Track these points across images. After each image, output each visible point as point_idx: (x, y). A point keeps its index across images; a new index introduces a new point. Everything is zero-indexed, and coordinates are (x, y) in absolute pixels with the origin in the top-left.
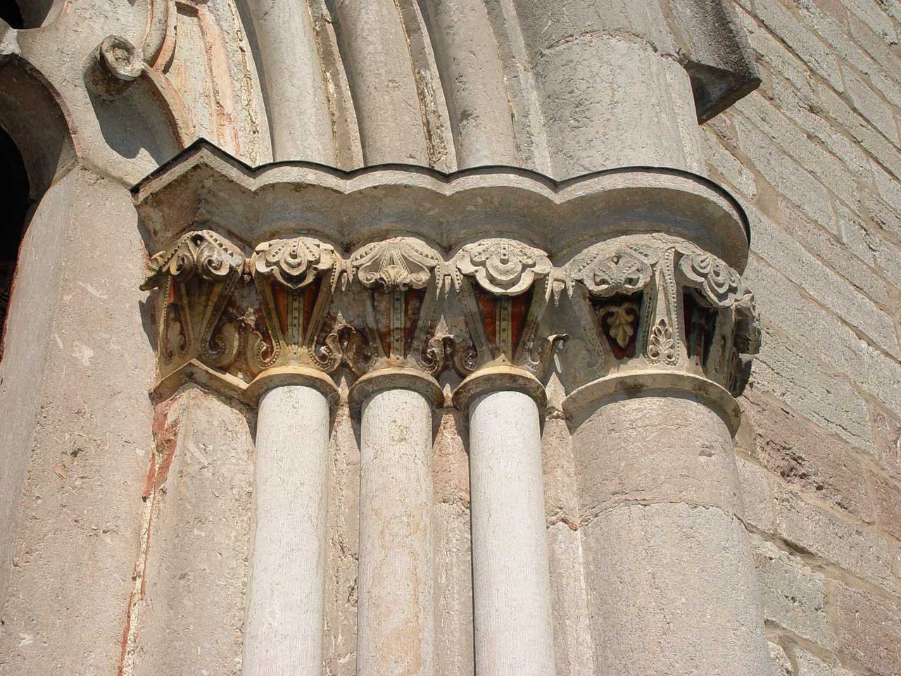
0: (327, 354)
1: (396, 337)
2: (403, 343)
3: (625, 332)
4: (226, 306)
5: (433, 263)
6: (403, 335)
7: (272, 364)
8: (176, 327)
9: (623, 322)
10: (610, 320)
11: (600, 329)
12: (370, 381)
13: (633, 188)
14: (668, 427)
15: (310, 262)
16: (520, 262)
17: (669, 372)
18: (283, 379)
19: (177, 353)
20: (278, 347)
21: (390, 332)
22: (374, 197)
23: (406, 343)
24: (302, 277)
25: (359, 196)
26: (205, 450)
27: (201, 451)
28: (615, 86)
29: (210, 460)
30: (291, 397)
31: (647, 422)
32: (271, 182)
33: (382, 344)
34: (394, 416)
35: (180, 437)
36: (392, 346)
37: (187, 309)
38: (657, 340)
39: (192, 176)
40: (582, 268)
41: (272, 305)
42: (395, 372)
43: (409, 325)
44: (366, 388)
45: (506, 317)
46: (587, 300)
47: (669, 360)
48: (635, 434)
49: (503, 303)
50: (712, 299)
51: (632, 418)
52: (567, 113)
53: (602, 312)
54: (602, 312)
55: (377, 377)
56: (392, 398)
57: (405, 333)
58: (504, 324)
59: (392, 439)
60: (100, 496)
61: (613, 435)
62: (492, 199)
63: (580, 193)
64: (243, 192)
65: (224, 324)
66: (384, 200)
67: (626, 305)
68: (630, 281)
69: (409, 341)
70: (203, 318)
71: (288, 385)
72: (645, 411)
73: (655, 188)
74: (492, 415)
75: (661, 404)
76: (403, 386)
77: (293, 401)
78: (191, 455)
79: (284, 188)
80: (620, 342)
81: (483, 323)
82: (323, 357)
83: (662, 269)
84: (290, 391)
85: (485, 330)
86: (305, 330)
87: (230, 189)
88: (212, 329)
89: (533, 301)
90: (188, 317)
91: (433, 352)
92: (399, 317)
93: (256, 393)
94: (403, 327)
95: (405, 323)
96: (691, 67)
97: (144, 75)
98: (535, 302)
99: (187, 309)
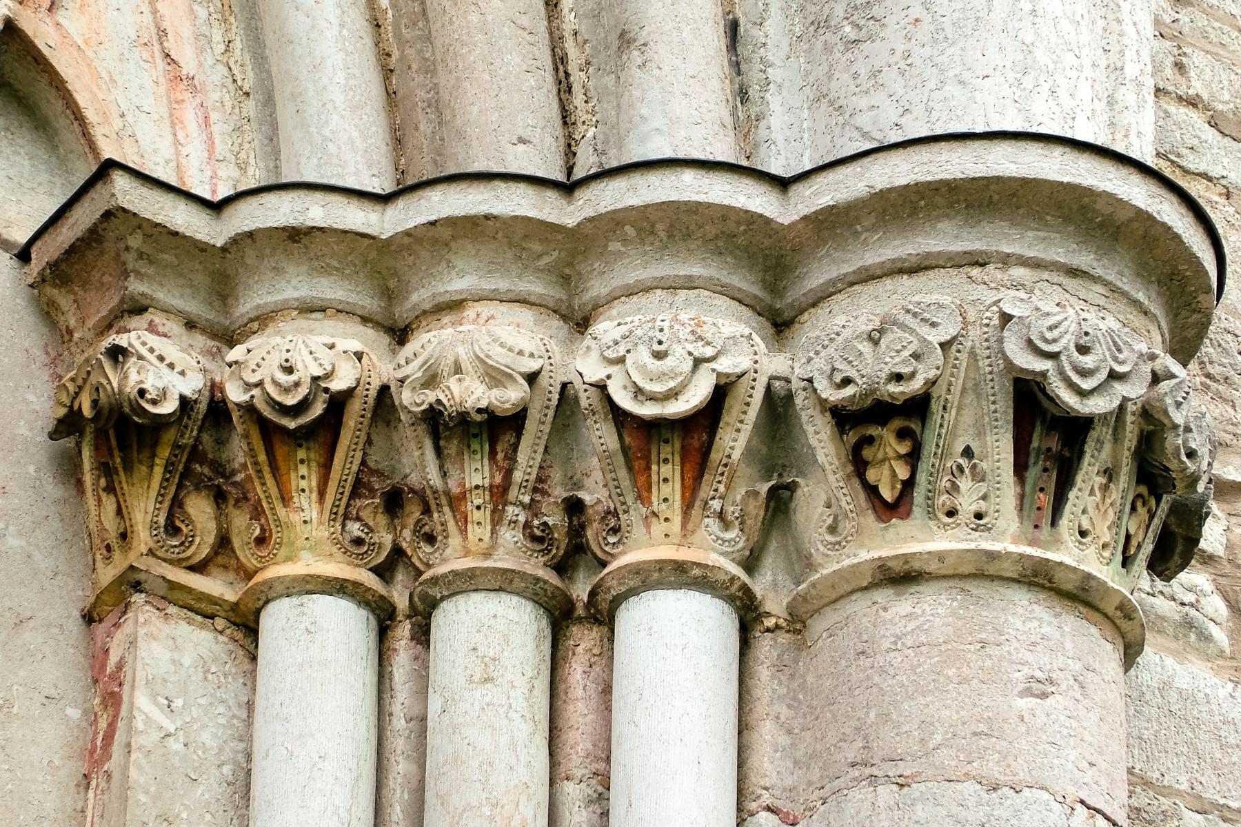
0: (363, 536)
1: (478, 502)
2: (488, 513)
3: (894, 474)
4: (189, 461)
6: (487, 498)
8: (109, 504)
9: (891, 454)
10: (867, 453)
11: (850, 468)
12: (434, 581)
13: (929, 182)
17: (972, 546)
18: (288, 585)
19: (116, 548)
20: (279, 529)
21: (465, 492)
22: (435, 241)
23: (493, 512)
25: (406, 240)
27: (162, 711)
29: (179, 723)
30: (304, 614)
31: (923, 638)
32: (246, 229)
33: (455, 517)
34: (473, 641)
35: (126, 688)
36: (469, 519)
37: (122, 473)
41: (262, 458)
42: (471, 565)
43: (498, 479)
45: (670, 457)
46: (828, 414)
47: (978, 522)
48: (899, 659)
49: (663, 431)
51: (898, 631)
53: (852, 437)
54: (852, 437)
55: (445, 576)
56: (471, 609)
57: (492, 496)
58: (666, 470)
59: (470, 680)
60: (9, 786)
61: (861, 663)
62: (653, 226)
63: (825, 200)
64: (202, 250)
65: (189, 492)
66: (453, 244)
67: (897, 423)
69: (500, 507)
70: (149, 487)
71: (300, 593)
72: (922, 619)
73: (974, 179)
74: (642, 633)
75: (955, 604)
76: (489, 587)
77: (306, 621)
78: (144, 717)
79: (270, 237)
80: (887, 494)
81: (630, 469)
82: (358, 542)
83: (972, 348)
85: (634, 482)
86: (322, 494)
87: (177, 248)
88: (166, 504)
89: (721, 425)
90: (125, 487)
91: (545, 524)
92: (480, 467)
93: (253, 606)
95: (492, 476)
98: (728, 424)
99: (122, 473)
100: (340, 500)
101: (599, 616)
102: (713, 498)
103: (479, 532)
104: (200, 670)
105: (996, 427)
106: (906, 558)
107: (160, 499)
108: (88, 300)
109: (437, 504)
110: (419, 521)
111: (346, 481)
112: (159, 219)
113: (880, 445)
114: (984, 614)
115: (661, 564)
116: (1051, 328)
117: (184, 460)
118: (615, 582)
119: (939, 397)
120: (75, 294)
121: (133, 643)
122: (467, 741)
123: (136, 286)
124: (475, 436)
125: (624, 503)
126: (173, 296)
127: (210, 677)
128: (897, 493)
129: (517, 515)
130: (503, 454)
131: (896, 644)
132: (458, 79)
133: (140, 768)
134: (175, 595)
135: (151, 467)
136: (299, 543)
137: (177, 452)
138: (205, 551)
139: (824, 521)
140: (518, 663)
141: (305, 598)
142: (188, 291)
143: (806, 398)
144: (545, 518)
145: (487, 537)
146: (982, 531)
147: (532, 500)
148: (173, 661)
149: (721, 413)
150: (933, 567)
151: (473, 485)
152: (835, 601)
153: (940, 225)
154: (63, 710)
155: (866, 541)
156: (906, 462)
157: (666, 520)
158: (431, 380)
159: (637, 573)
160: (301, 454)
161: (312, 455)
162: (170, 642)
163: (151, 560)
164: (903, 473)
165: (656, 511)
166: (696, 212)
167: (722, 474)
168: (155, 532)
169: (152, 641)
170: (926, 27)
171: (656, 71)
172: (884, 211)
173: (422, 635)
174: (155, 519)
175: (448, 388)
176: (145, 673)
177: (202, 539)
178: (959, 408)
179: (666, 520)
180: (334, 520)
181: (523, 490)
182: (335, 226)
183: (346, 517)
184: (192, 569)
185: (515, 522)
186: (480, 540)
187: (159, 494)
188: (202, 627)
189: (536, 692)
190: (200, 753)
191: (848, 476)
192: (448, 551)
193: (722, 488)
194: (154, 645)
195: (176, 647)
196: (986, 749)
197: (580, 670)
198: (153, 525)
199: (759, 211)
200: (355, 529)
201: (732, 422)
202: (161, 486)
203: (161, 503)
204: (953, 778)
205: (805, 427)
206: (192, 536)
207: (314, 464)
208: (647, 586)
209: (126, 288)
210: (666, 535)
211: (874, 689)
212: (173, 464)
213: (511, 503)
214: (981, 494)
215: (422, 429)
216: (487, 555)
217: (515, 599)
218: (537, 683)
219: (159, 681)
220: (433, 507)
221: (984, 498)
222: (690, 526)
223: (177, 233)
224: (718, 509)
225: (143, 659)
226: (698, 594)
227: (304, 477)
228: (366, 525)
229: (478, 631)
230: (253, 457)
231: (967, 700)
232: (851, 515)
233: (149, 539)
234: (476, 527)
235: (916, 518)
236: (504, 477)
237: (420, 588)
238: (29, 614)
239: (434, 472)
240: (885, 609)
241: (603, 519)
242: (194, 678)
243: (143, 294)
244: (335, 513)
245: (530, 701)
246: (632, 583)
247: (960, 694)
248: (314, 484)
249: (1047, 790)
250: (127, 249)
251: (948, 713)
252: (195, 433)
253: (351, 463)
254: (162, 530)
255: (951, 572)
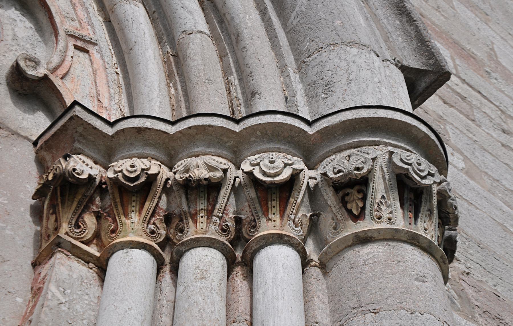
0: (155, 230)
1: (202, 214)
3: (357, 205)
5: (226, 167)
7: (117, 237)
8: (53, 218)
10: (347, 198)
11: (341, 205)
12: (183, 244)
14: (391, 263)
15: (143, 170)
16: (283, 162)
20: (121, 226)
23: (208, 219)
24: (137, 178)
25: (180, 135)
26: (64, 292)
27: (61, 293)
28: (350, 72)
29: (67, 299)
31: (375, 260)
34: (197, 264)
36: (198, 221)
37: (60, 205)
38: (381, 209)
39: (69, 125)
40: (325, 166)
41: (118, 200)
43: (210, 208)
44: (181, 249)
46: (331, 187)
48: (367, 268)
50: (415, 179)
51: (365, 258)
52: (320, 91)
53: (341, 194)
54: (341, 194)
56: (197, 253)
58: (274, 203)
62: (267, 132)
64: (104, 137)
66: (196, 136)
67: (357, 187)
68: (358, 169)
74: (266, 261)
75: (385, 248)
76: (205, 245)
77: (129, 258)
78: (52, 294)
80: (355, 212)
81: (260, 204)
84: (128, 252)
85: (262, 209)
89: (294, 189)
91: (227, 225)
92: (203, 202)
94: (205, 209)
95: (208, 206)
96: (404, 69)
97: (46, 76)
98: (296, 189)
99: (60, 205)
100: (147, 216)
101: (246, 262)
102: (291, 214)
104: (80, 280)
105: (392, 189)
106: (365, 232)
107: (74, 214)
108: (58, 155)
109: (186, 217)
110: (177, 224)
111: (150, 209)
112: (90, 122)
113: (351, 195)
114: (397, 252)
116: (407, 156)
117: (86, 201)
118: (254, 244)
119: (371, 179)
120: (53, 153)
121: (53, 266)
122: (194, 301)
123: (77, 145)
124: (202, 192)
125: (258, 216)
126: (91, 152)
127: (84, 284)
128: (359, 212)
129: (217, 220)
130: (212, 200)
131: (365, 263)
132: (198, 103)
133: (46, 314)
135: (72, 202)
136: (128, 231)
137: (84, 197)
138: (89, 236)
139: (332, 225)
140: (215, 273)
141: (129, 250)
142: (96, 151)
143: (323, 184)
144: (227, 223)
145: (204, 228)
146: (391, 224)
147: (222, 216)
148: (69, 275)
149: (293, 186)
150: (376, 235)
151: (200, 208)
152: (338, 253)
153: (363, 133)
154: (15, 298)
155: (349, 230)
156: (362, 201)
157: (274, 221)
158: (187, 171)
159: (264, 239)
160: (134, 198)
161: (138, 199)
162: (69, 268)
163: (66, 236)
164: (361, 205)
165: (270, 218)
166: (281, 127)
167: (294, 206)
168: (70, 226)
169: (61, 266)
171: (264, 99)
172: (345, 129)
173: (175, 271)
174: (71, 221)
175: (194, 172)
176: (56, 277)
177: (89, 231)
179: (274, 221)
180: (144, 223)
181: (219, 211)
182: (154, 128)
184: (82, 242)
185: (216, 223)
186: (202, 229)
187: (74, 212)
188: (84, 265)
189: (222, 285)
190: (74, 313)
191: (340, 207)
192: (189, 233)
193: (294, 211)
194: (62, 267)
195: (71, 270)
196: (407, 298)
197: (239, 281)
199: (302, 128)
200: (152, 227)
201: (297, 189)
202: (75, 209)
203: (74, 215)
204: (396, 309)
205: (323, 193)
206: (85, 230)
207: (138, 202)
208: (267, 245)
209: (73, 146)
210: (274, 227)
211: (359, 279)
212: (81, 202)
213: (215, 216)
214: (389, 211)
215: (181, 191)
217: (215, 250)
218: (222, 282)
219: (61, 281)
220: (184, 218)
221: (391, 213)
222: (283, 223)
223: (96, 128)
224: (293, 218)
225: (56, 271)
226: (287, 247)
228: (156, 226)
229: (200, 261)
230: (114, 200)
231: (396, 280)
232: (342, 221)
233: (67, 228)
234: (201, 224)
235: (367, 220)
236: (212, 207)
237: (176, 248)
238: (9, 259)
239: (185, 206)
240: (359, 252)
241: (249, 223)
242: (77, 283)
243: (79, 148)
244: (145, 220)
245: (220, 288)
246: (261, 244)
247: (393, 278)
248: (138, 209)
249: (433, 315)
250: (76, 132)
251: (389, 285)
252: (92, 192)
253: (153, 203)
254: (73, 225)
255: (382, 237)
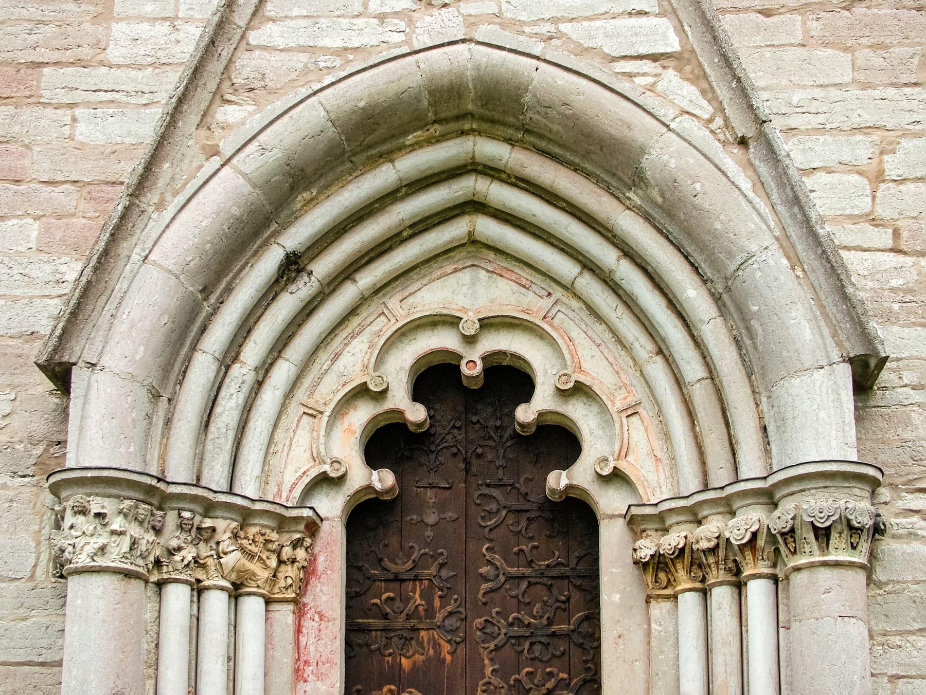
80: (792, 550)
86: (684, 568)
103: (715, 572)
115: (750, 575)
134: (659, 597)
170: (794, 429)
178: (801, 529)
183: (690, 572)
184: (663, 589)
198: (652, 582)
216: (717, 578)
227: (679, 566)
